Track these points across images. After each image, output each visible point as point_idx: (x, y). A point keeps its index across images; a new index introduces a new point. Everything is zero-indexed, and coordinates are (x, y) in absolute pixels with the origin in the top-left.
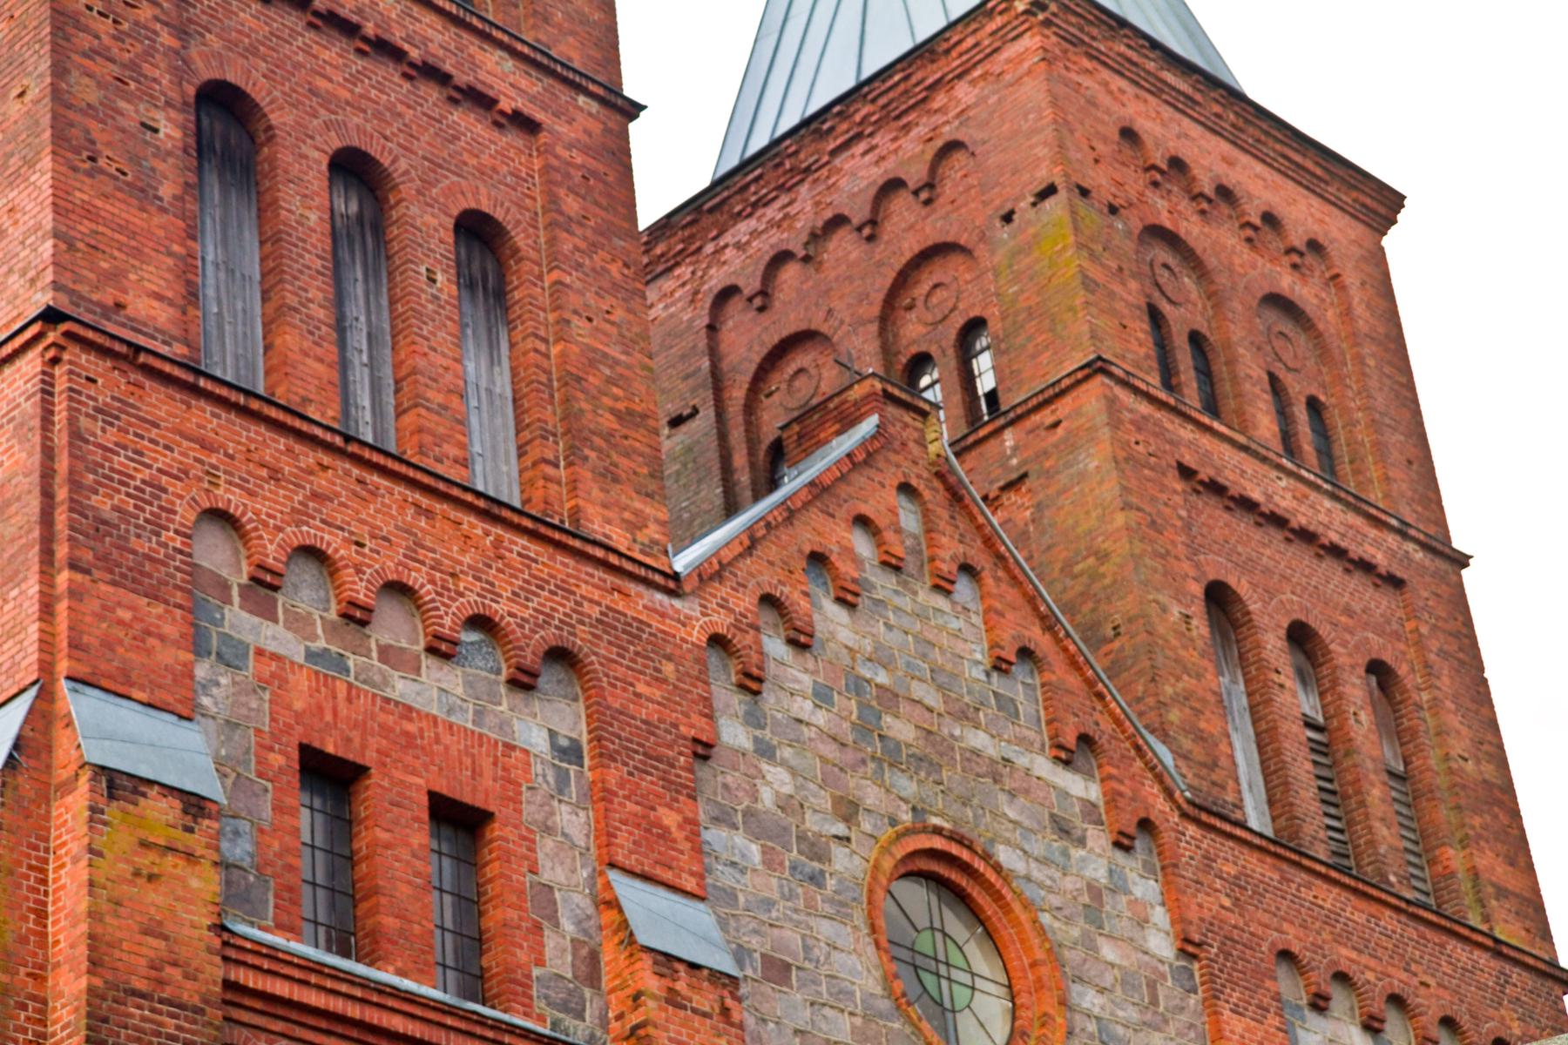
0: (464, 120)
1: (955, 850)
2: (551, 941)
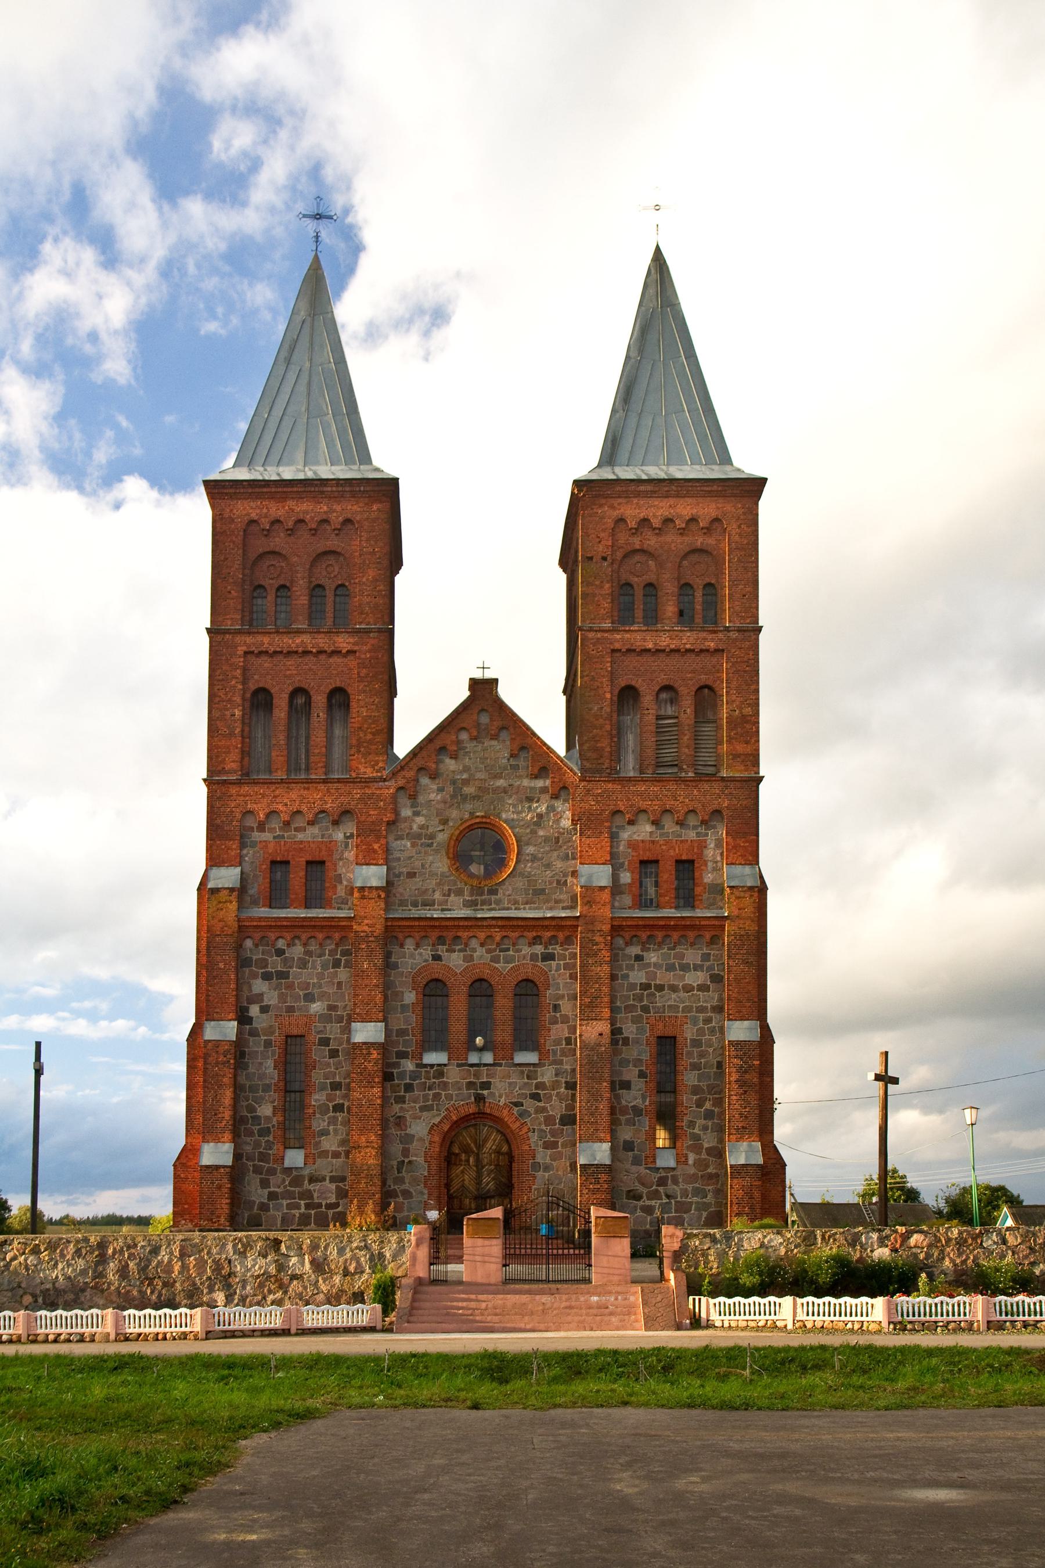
0: (335, 660)
1: (484, 820)
2: (339, 887)
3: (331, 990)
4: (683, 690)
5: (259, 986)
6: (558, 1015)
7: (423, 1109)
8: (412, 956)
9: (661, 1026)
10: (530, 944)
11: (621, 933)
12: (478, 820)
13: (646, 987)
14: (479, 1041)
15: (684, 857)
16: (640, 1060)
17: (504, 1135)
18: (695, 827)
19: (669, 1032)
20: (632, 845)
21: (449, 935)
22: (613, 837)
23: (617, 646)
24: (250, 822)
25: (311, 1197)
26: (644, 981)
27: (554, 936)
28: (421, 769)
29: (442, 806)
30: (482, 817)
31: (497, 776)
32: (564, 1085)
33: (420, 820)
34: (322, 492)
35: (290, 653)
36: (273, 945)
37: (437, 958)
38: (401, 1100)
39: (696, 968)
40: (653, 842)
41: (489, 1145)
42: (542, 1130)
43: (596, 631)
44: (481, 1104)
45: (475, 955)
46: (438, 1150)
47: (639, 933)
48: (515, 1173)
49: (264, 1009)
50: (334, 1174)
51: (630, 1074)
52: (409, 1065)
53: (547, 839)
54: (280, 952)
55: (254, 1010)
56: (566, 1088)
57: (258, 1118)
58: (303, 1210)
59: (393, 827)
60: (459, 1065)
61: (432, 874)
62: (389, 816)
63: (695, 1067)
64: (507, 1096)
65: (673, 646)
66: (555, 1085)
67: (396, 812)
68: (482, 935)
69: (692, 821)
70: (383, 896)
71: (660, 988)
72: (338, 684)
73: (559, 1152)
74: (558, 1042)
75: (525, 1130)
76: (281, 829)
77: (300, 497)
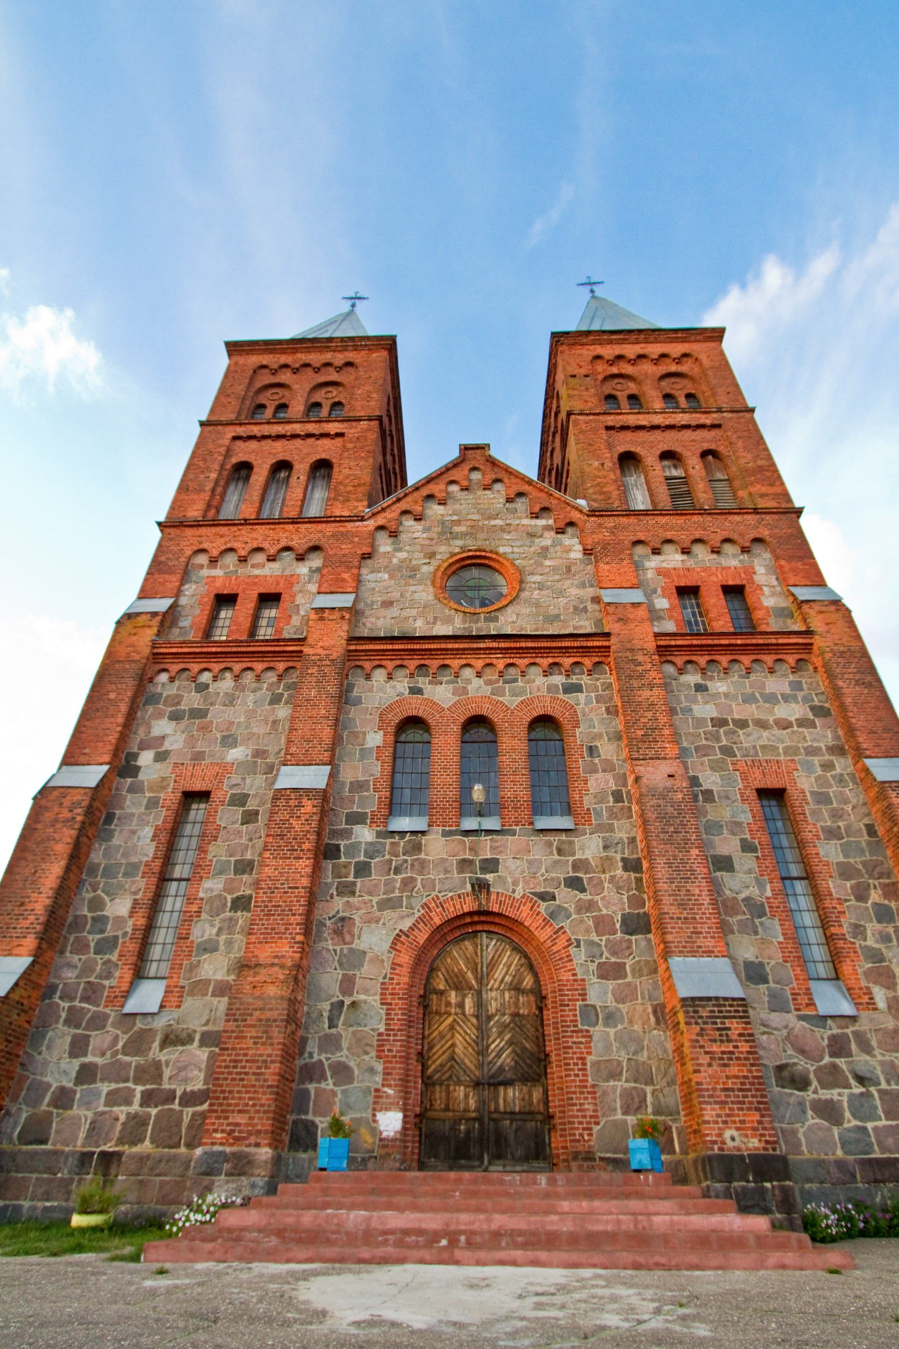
1: (478, 553)
3: (260, 729)
4: (685, 453)
5: (162, 727)
6: (596, 760)
7: (385, 905)
8: (382, 690)
9: (757, 774)
10: (546, 674)
11: (669, 658)
12: (470, 554)
13: (720, 722)
14: (478, 792)
15: (731, 583)
16: (739, 824)
17: (526, 956)
18: (734, 556)
19: (772, 783)
20: (660, 572)
21: (434, 664)
22: (638, 567)
23: (610, 424)
24: (202, 559)
25: (158, 1077)
26: (715, 714)
27: (576, 663)
28: (405, 512)
29: (427, 542)
30: (476, 551)
31: (490, 518)
32: (620, 864)
33: (402, 555)
34: (328, 347)
35: (279, 437)
36: (194, 679)
37: (416, 691)
38: (347, 890)
39: (786, 698)
40: (688, 569)
41: (499, 973)
42: (592, 943)
43: (587, 414)
44: (483, 897)
45: (469, 687)
46: (406, 979)
47: (693, 658)
48: (550, 1031)
49: (161, 757)
50: (210, 1028)
51: (727, 845)
52: (365, 834)
53: (555, 569)
54: (202, 688)
55: (146, 758)
56: (626, 869)
57: (103, 920)
58: (135, 1107)
59: (368, 562)
60: (445, 834)
61: (413, 604)
62: (367, 550)
63: (832, 834)
64: (526, 882)
65: (667, 423)
66: (606, 864)
67: (372, 545)
68: (479, 664)
69: (728, 548)
70: (347, 616)
71: (742, 724)
72: (323, 456)
73: (629, 985)
74: (600, 797)
75: (561, 942)
76: (235, 566)
77: (308, 350)
